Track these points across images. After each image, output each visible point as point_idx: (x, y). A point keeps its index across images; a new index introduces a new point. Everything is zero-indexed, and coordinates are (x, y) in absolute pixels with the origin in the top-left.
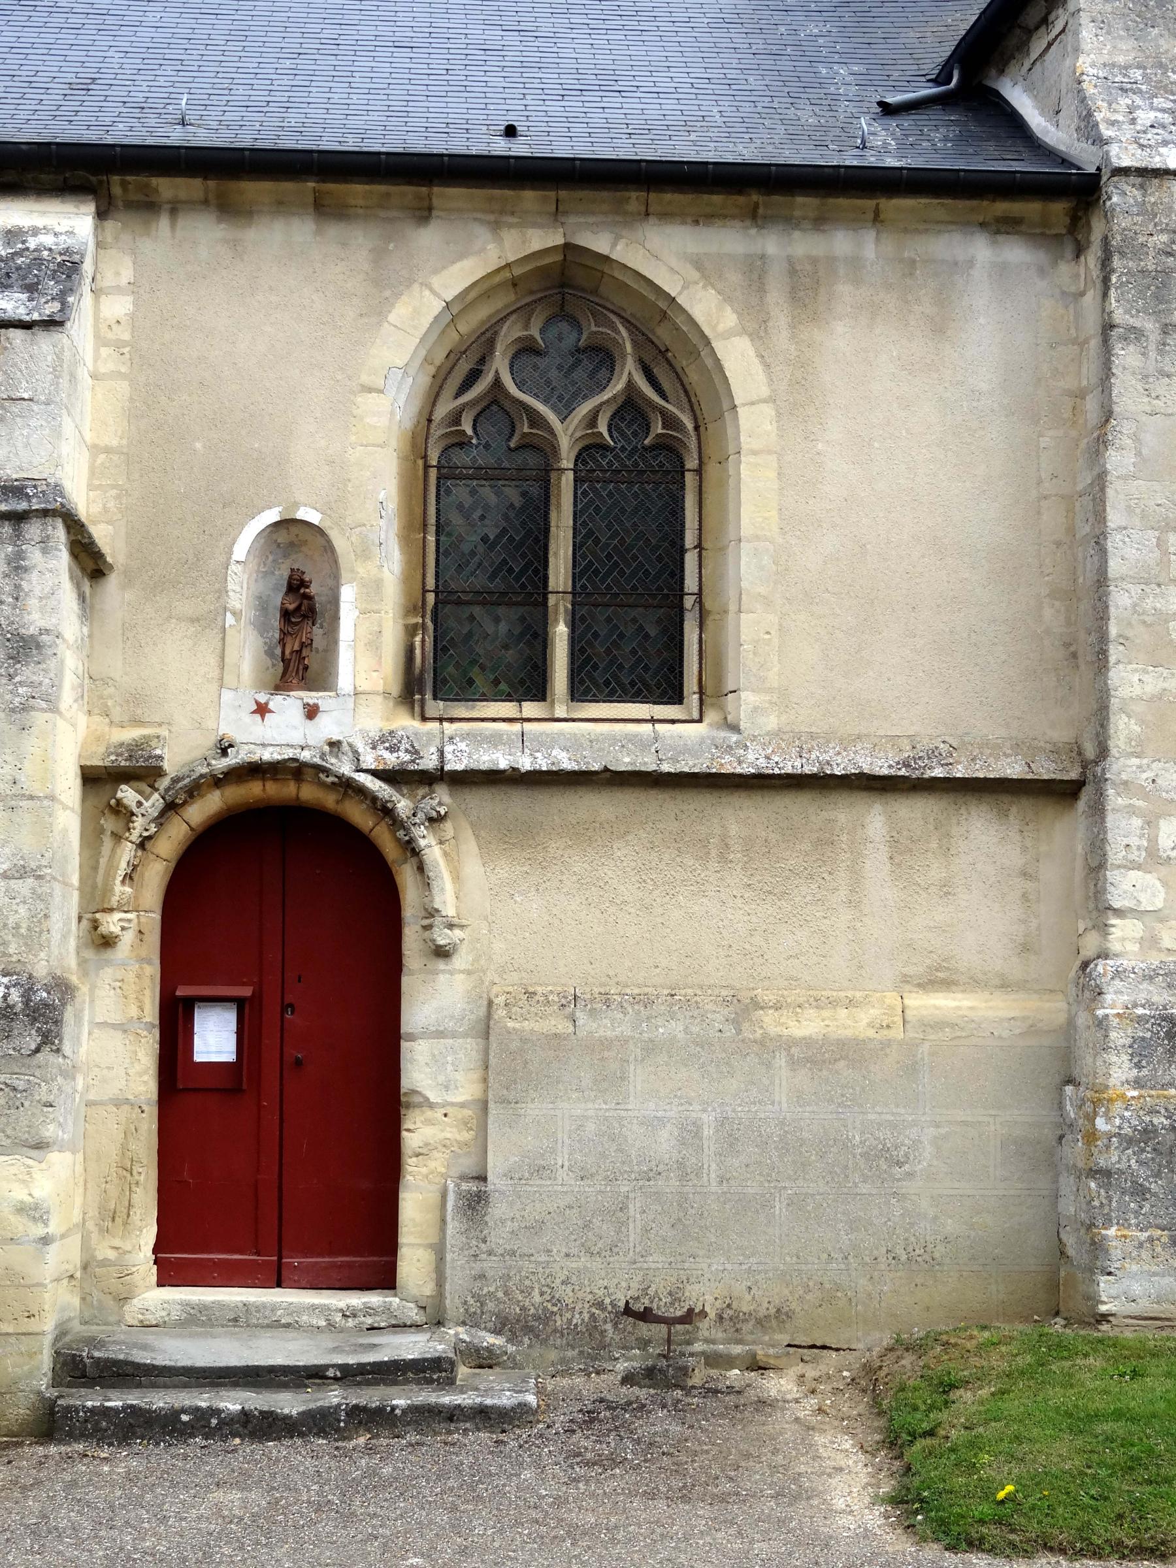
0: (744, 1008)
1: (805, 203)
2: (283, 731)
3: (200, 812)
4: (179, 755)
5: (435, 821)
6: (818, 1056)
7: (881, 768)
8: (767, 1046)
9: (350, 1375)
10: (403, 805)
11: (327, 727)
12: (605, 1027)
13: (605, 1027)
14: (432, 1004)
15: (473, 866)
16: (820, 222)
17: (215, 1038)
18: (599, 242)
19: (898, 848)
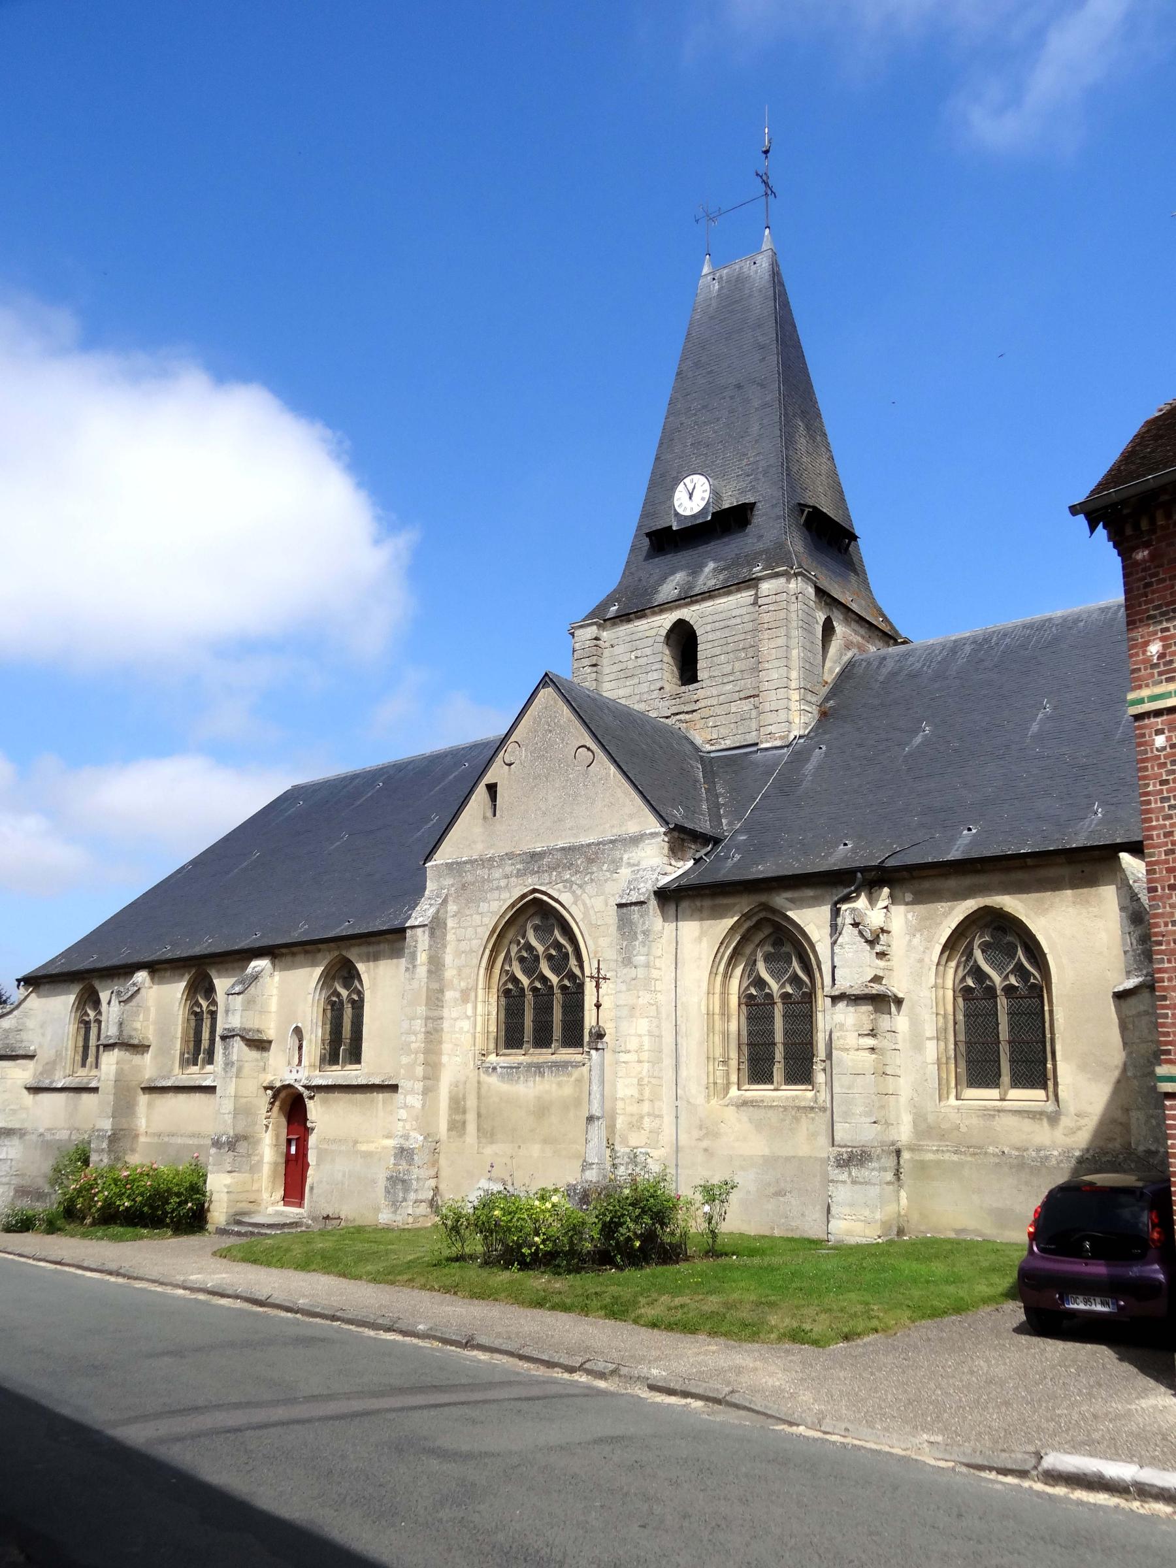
0: (356, 1142)
1: (373, 939)
2: (289, 1079)
3: (283, 1095)
4: (278, 1084)
5: (311, 1098)
6: (367, 1155)
7: (377, 1081)
8: (357, 1152)
9: (270, 1226)
10: (306, 1093)
11: (298, 1076)
12: (334, 1147)
13: (334, 1147)
14: (312, 1140)
15: (319, 1108)
16: (379, 943)
17: (293, 1150)
18: (344, 953)
19: (384, 1102)
